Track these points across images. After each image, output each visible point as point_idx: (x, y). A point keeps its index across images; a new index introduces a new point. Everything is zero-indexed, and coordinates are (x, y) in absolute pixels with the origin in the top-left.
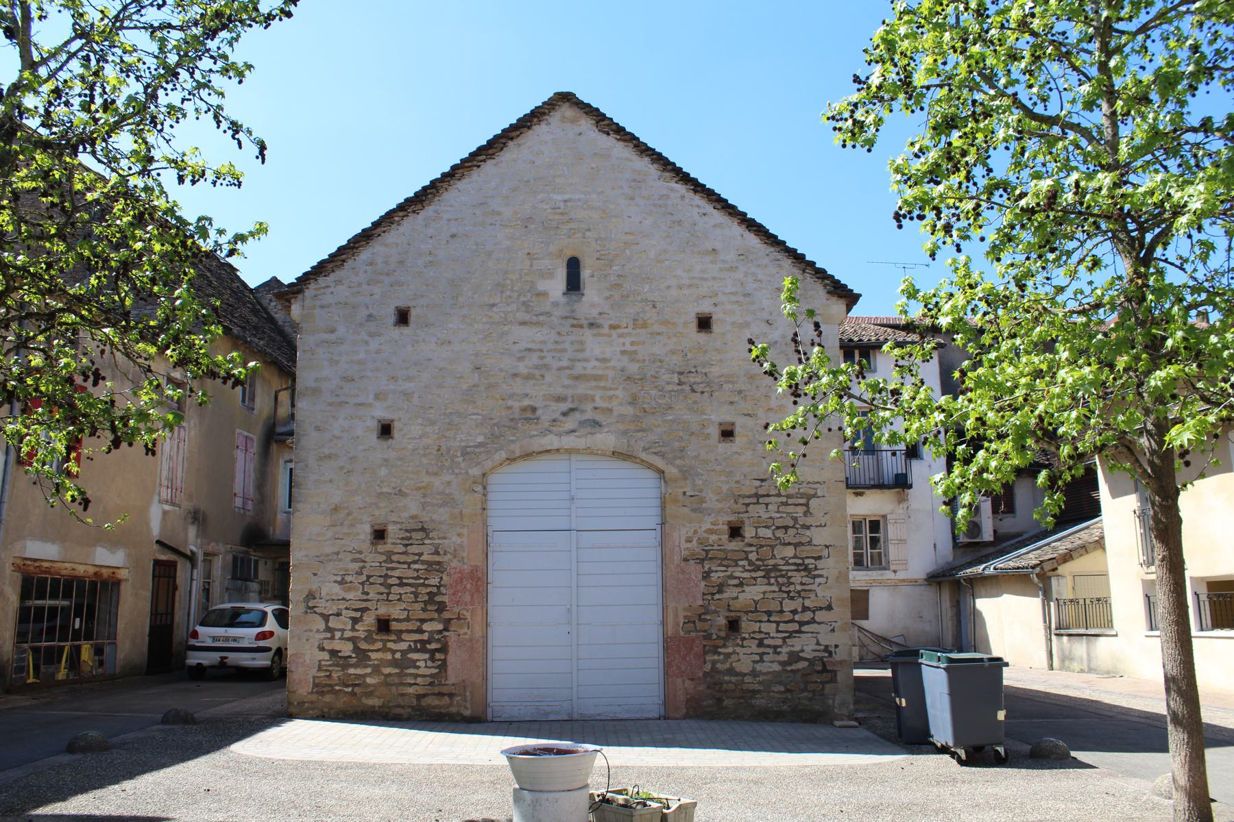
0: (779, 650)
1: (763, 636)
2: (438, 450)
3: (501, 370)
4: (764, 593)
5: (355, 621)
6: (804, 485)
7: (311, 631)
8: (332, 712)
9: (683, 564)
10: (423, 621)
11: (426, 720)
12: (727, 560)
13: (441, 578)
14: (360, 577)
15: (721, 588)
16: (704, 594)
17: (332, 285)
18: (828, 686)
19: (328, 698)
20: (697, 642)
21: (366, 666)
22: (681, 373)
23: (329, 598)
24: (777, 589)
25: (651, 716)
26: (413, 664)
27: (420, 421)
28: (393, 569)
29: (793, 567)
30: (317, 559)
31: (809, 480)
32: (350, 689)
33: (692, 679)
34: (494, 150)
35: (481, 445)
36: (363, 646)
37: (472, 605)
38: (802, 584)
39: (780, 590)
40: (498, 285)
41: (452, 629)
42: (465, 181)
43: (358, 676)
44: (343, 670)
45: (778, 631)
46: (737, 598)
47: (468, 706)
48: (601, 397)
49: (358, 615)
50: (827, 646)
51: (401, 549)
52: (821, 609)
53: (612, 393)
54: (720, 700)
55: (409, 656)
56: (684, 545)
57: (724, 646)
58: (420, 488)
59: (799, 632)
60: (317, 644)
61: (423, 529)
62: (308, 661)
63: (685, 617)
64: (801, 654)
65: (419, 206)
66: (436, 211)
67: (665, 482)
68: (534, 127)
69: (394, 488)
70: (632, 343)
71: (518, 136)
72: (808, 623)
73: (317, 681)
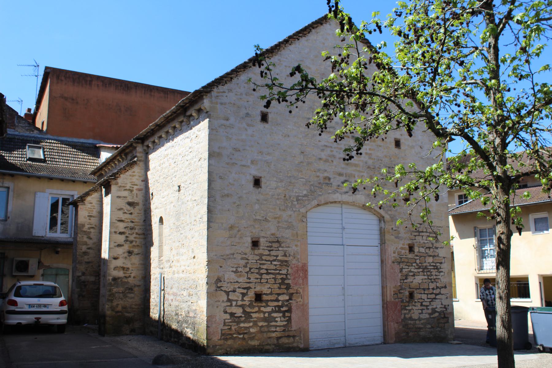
0: (428, 307)
1: (422, 301)
2: (285, 197)
3: (314, 155)
4: (422, 279)
5: (244, 295)
6: (436, 228)
7: (219, 301)
8: (232, 350)
9: (392, 264)
10: (279, 294)
11: (282, 352)
12: (409, 263)
13: (288, 270)
14: (245, 269)
15: (406, 277)
16: (401, 280)
17: (227, 91)
19: (230, 342)
20: (399, 304)
21: (250, 322)
22: (389, 168)
24: (427, 278)
25: (378, 342)
27: (275, 179)
28: (264, 264)
29: (432, 267)
31: (438, 225)
32: (241, 336)
33: (397, 323)
34: (307, 32)
35: (305, 196)
36: (248, 310)
37: (303, 285)
38: (436, 275)
39: (428, 278)
40: (311, 108)
41: (293, 299)
42: (293, 46)
44: (237, 325)
45: (428, 298)
46: (412, 282)
47: (302, 342)
48: (358, 176)
49: (245, 291)
50: (445, 306)
51: (267, 252)
52: (443, 287)
53: (362, 174)
54: (408, 333)
55: (273, 315)
56: (393, 255)
57: (408, 306)
58: (276, 218)
59: (435, 298)
60: (223, 309)
61: (278, 242)
62: (218, 320)
63: (394, 291)
64: (436, 309)
65: (270, 55)
66: (279, 60)
67: (384, 222)
68: (324, 25)
70: (370, 149)
71: (316, 27)
72: (438, 294)
73: (223, 332)
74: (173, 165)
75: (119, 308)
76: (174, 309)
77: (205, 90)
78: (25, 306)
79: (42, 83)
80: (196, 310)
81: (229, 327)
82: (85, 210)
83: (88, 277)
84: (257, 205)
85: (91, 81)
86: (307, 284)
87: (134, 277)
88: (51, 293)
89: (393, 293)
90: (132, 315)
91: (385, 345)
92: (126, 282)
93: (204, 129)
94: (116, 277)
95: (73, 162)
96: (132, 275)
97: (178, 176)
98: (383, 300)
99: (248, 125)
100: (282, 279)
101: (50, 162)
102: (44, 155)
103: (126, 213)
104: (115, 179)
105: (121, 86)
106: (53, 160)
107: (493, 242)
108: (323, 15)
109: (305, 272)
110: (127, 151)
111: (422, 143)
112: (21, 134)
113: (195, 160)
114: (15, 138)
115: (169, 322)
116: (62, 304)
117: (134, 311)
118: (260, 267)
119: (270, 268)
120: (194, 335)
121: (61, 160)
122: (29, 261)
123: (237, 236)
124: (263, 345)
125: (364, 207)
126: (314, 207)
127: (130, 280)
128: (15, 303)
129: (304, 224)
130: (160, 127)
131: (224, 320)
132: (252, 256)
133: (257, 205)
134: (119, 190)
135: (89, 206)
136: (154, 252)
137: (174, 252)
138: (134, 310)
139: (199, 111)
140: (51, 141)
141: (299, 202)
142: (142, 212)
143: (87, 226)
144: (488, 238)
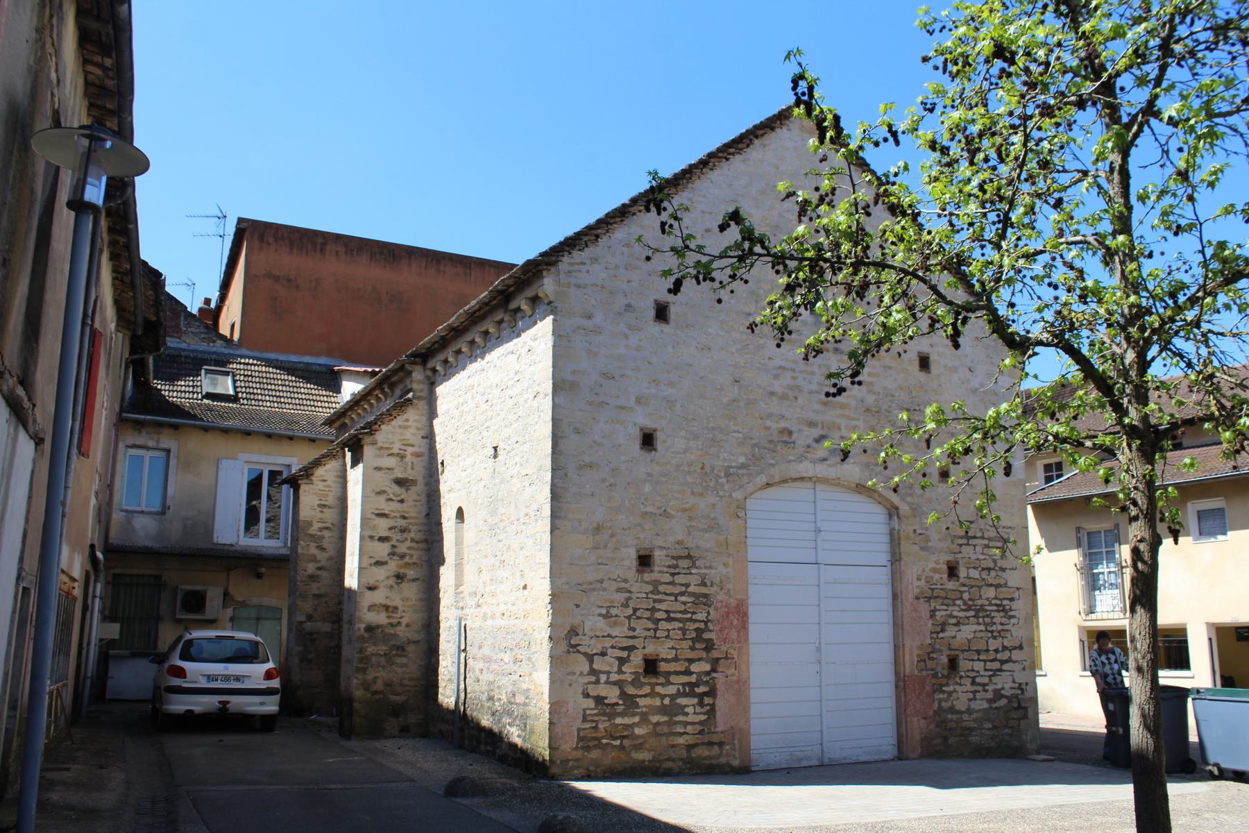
2: (702, 468)
3: (759, 386)
4: (975, 632)
5: (622, 661)
7: (574, 674)
10: (691, 661)
12: (948, 600)
13: (709, 613)
14: (625, 610)
15: (943, 627)
17: (588, 262)
18: (1022, 722)
19: (594, 754)
21: (634, 715)
23: (592, 634)
25: (886, 757)
26: (681, 710)
27: (683, 433)
28: (660, 601)
29: (995, 608)
30: (579, 587)
32: (618, 742)
33: (925, 718)
34: (744, 146)
35: (743, 466)
36: (631, 690)
37: (739, 642)
38: (1002, 624)
39: (986, 630)
41: (720, 670)
42: (717, 172)
43: (626, 726)
44: (609, 720)
45: (986, 670)
46: (955, 637)
47: (737, 755)
49: (624, 654)
50: (1020, 684)
51: (667, 578)
52: (1015, 648)
53: (854, 423)
54: (946, 739)
55: (679, 701)
57: (947, 685)
58: (685, 510)
59: (1001, 670)
61: (689, 557)
62: (571, 710)
63: (918, 656)
64: (1003, 692)
65: (673, 190)
66: (690, 199)
67: (899, 517)
68: (778, 130)
69: (660, 508)
71: (762, 135)
73: (582, 734)
74: (483, 407)
75: (379, 686)
76: (484, 688)
77: (546, 259)
78: (201, 678)
79: (231, 250)
80: (528, 690)
81: (594, 725)
82: (314, 494)
83: (319, 624)
84: (647, 485)
85: (324, 244)
86: (747, 640)
87: (407, 625)
88: (249, 655)
89: (916, 659)
91: (900, 762)
92: (391, 634)
93: (543, 336)
95: (290, 400)
96: (404, 621)
97: (493, 428)
98: (897, 673)
99: (630, 328)
100: (697, 630)
101: (245, 402)
102: (235, 388)
103: (391, 500)
104: (371, 434)
105: (381, 253)
106: (252, 397)
107: (1114, 558)
108: (776, 111)
109: (743, 617)
110: (394, 379)
111: (972, 361)
112: (193, 347)
113: (526, 396)
114: (181, 356)
115: (475, 713)
116: (269, 675)
117: (408, 691)
118: (654, 607)
119: (674, 609)
120: (524, 740)
121: (267, 398)
122: (205, 592)
123: (609, 545)
124: (659, 761)
125: (860, 488)
126: (760, 489)
127: (401, 631)
128: (181, 673)
129: (740, 521)
130: (457, 332)
131: (584, 710)
132: (638, 584)
133: (647, 485)
134: (380, 456)
135: (321, 485)
136: (447, 575)
137: (485, 576)
138: (407, 688)
139: (535, 300)
140: (247, 361)
141: (731, 478)
142: (423, 498)
143: (316, 526)
144: (1104, 550)
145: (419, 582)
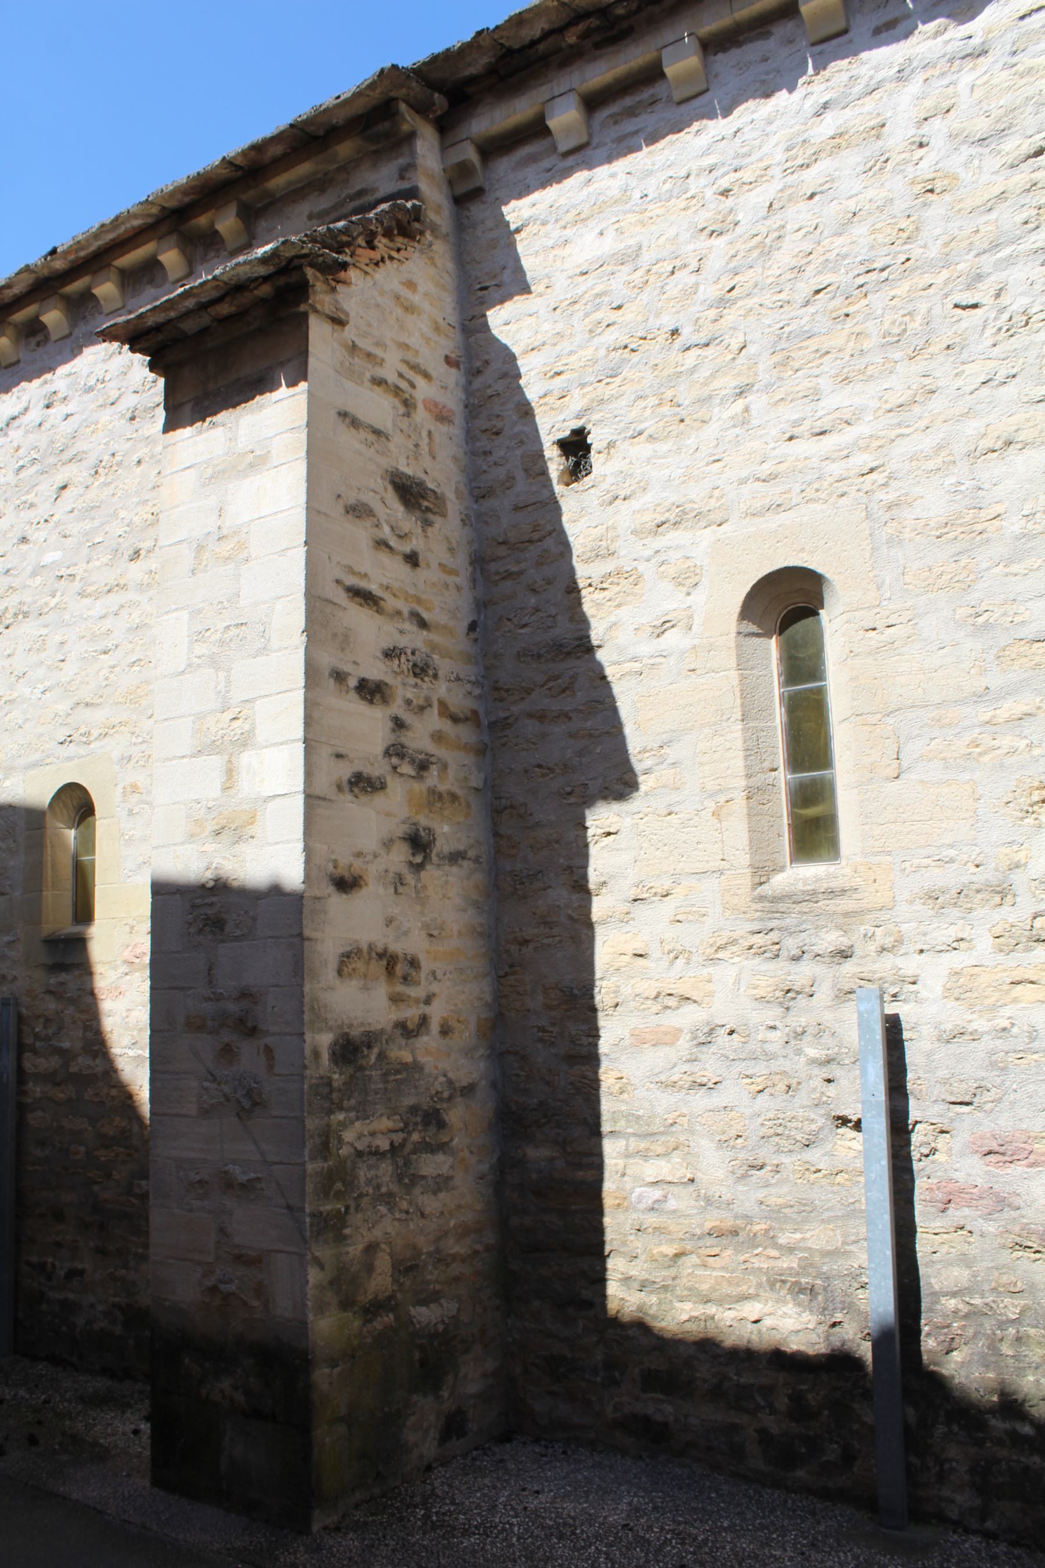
90: (449, 1307)
92: (405, 1066)
94: (355, 1033)
96: (437, 1012)
138: (456, 1269)
145: (465, 863)
